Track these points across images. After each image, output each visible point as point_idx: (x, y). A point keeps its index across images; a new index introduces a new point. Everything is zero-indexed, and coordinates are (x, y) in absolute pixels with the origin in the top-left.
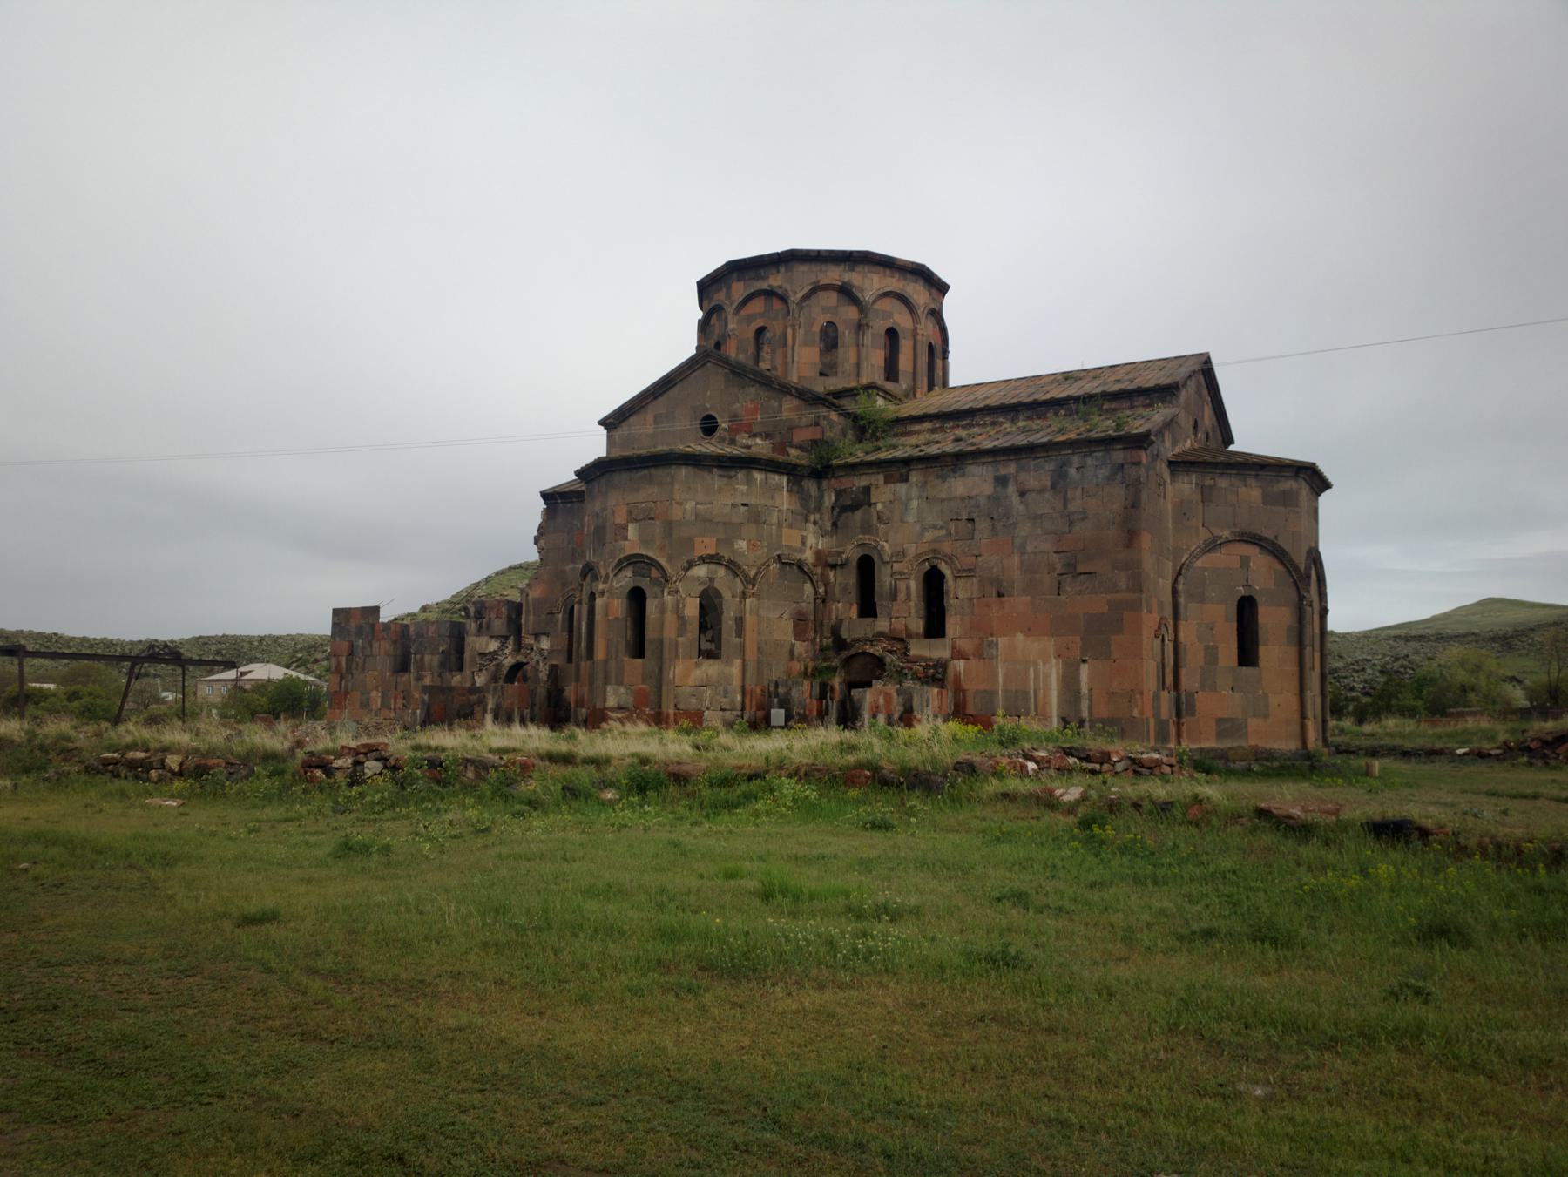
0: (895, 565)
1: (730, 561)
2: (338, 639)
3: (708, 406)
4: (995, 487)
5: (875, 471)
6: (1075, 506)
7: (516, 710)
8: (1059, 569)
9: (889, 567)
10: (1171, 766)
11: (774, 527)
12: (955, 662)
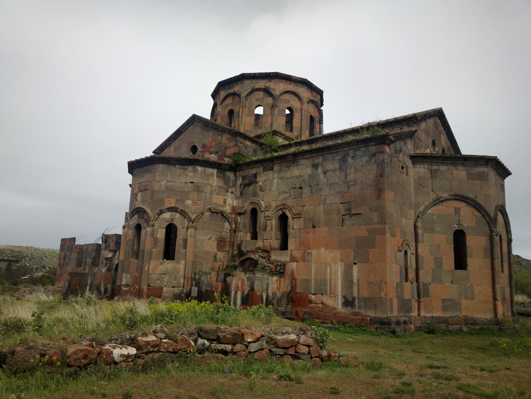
0: (266, 212)
1: (181, 210)
2: (61, 252)
3: (194, 141)
4: (312, 170)
5: (259, 166)
6: (351, 177)
7: (102, 285)
8: (343, 212)
9: (263, 213)
10: (309, 346)
11: (208, 194)
12: (292, 263)
